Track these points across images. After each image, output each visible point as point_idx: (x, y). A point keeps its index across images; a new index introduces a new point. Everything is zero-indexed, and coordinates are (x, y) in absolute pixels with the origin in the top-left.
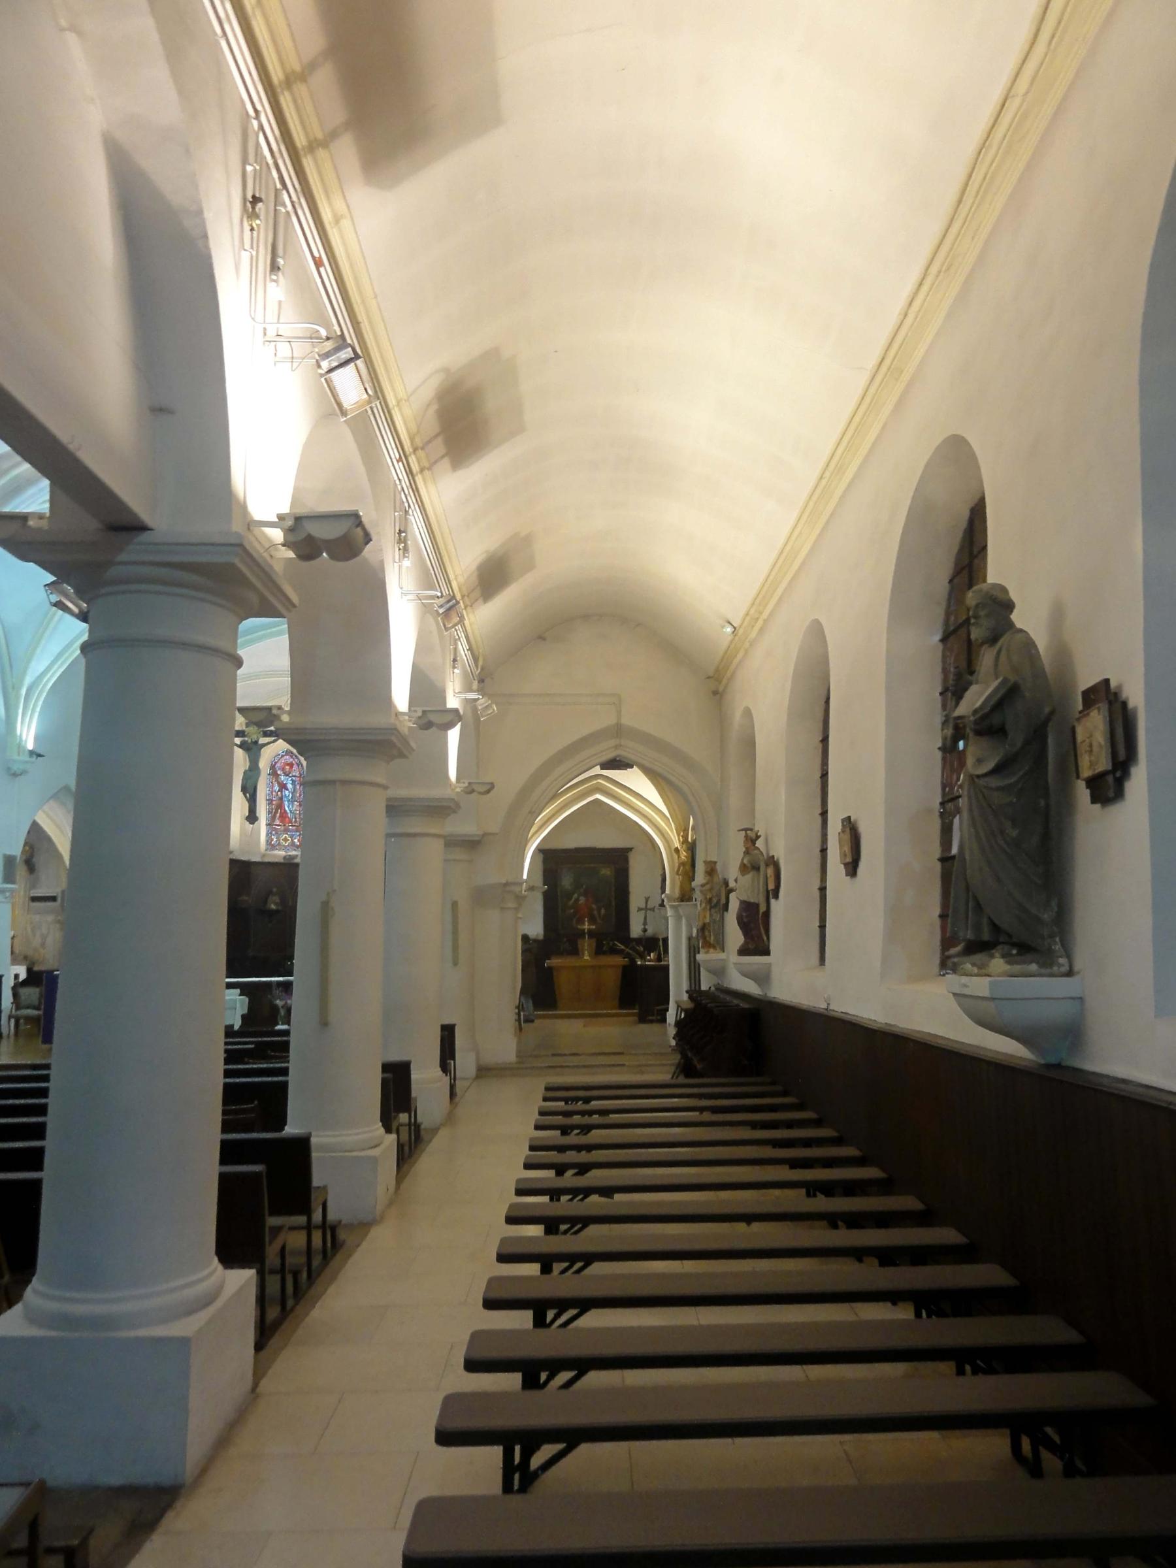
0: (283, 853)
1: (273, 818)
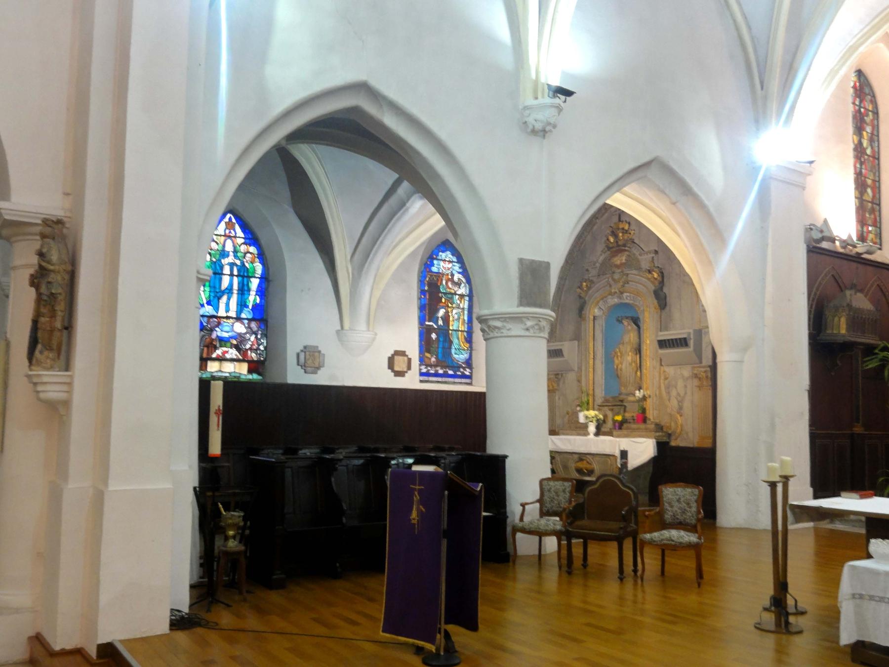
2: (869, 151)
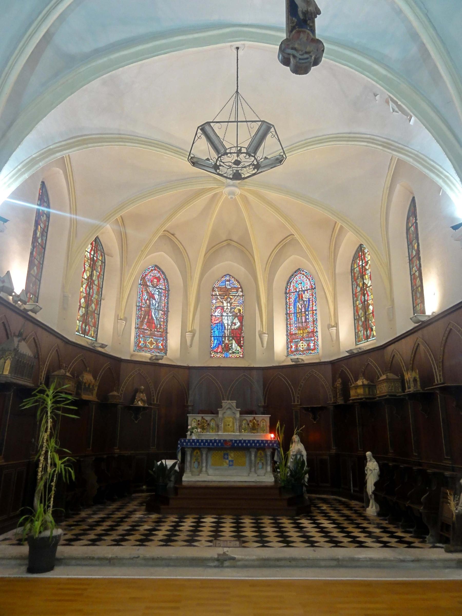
0: (148, 355)
1: (142, 322)
2: (40, 241)
